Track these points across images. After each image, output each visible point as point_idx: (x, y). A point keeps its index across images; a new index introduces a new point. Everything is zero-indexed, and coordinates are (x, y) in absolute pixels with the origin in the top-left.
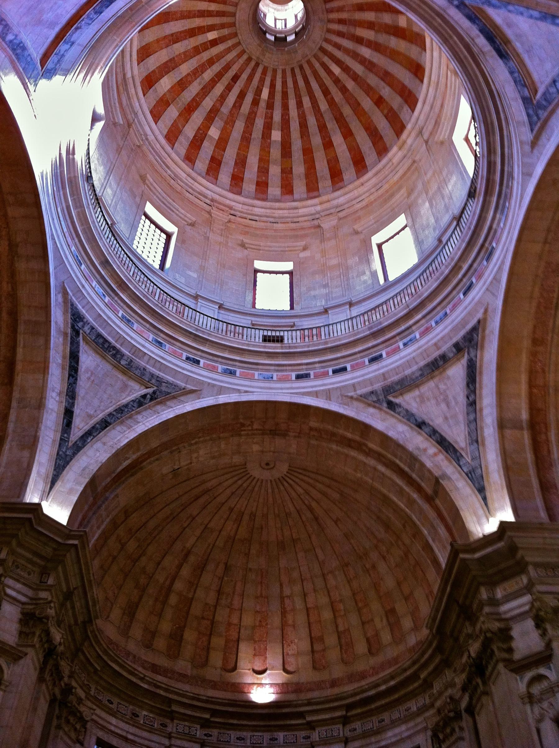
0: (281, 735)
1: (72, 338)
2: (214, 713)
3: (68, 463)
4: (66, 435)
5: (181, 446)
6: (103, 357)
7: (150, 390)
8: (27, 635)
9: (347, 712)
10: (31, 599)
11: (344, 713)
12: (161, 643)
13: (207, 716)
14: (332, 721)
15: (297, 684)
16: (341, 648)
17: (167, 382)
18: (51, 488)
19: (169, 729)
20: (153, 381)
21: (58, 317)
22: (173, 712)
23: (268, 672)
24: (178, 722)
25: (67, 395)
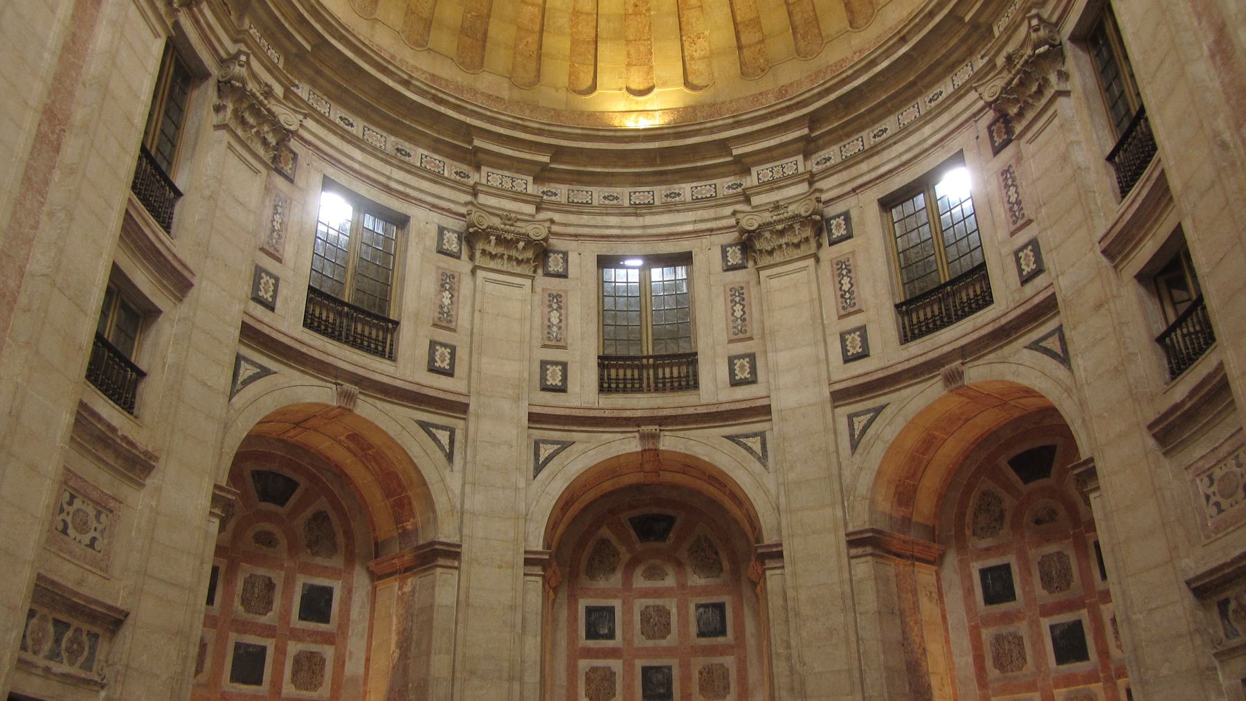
0: (686, 190)
2: (558, 153)
9: (811, 130)
11: (806, 131)
12: (444, 40)
13: (546, 159)
14: (782, 151)
15: (712, 105)
16: (794, 33)
19: (474, 178)
22: (478, 150)
23: (656, 91)
24: (490, 169)
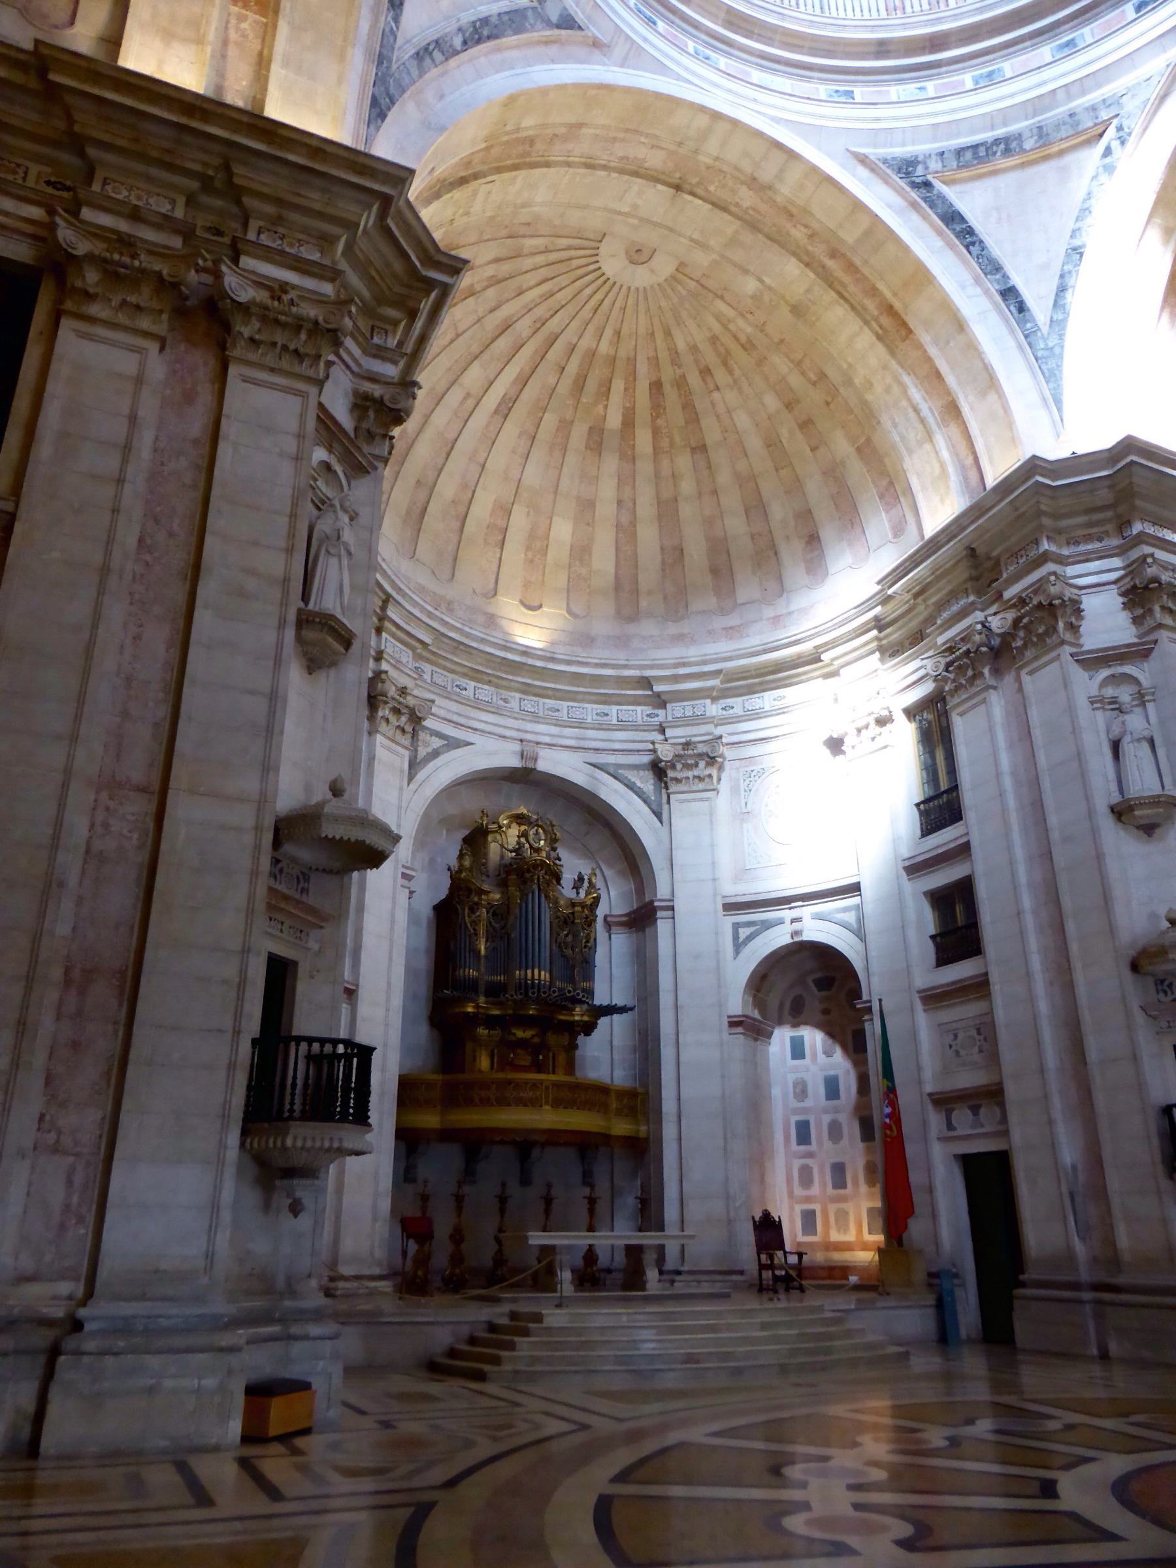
1: (925, 199)
4: (1029, 325)
8: (1143, 616)
10: (1123, 568)
18: (1060, 410)
21: (882, 201)
25: (986, 274)
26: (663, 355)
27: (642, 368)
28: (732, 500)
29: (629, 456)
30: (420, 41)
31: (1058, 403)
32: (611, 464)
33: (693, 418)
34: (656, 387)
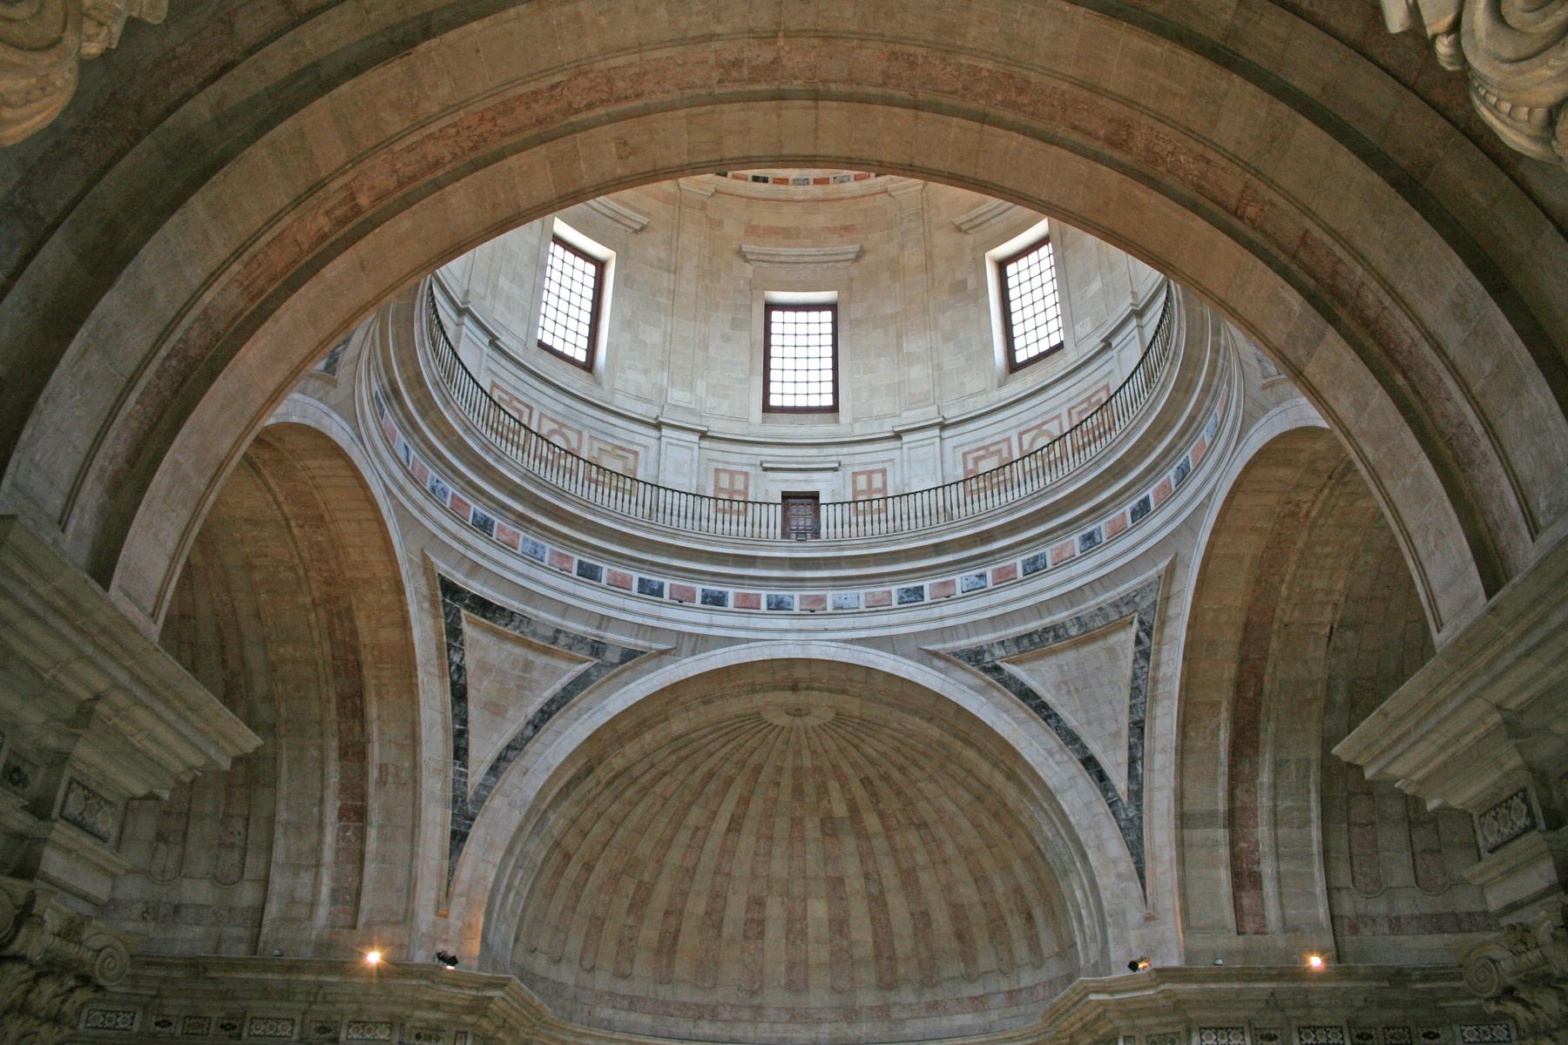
3: (1141, 829)
5: (1278, 612)
6: (1053, 652)
7: (1136, 624)
17: (1138, 592)
20: (1125, 610)
26: (862, 761)
27: (847, 770)
28: (960, 869)
29: (863, 835)
30: (490, 756)
31: (1142, 877)
32: (849, 844)
33: (908, 804)
34: (866, 782)
